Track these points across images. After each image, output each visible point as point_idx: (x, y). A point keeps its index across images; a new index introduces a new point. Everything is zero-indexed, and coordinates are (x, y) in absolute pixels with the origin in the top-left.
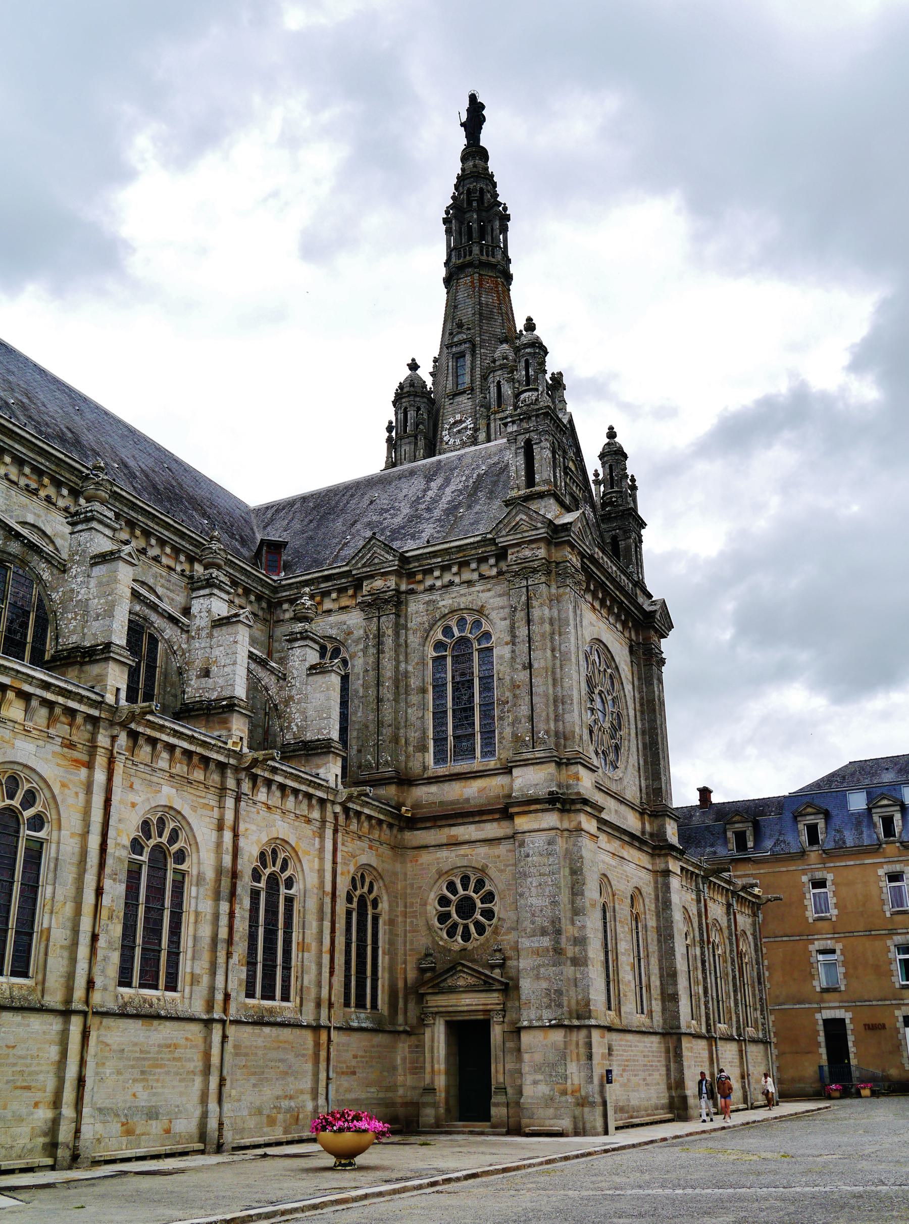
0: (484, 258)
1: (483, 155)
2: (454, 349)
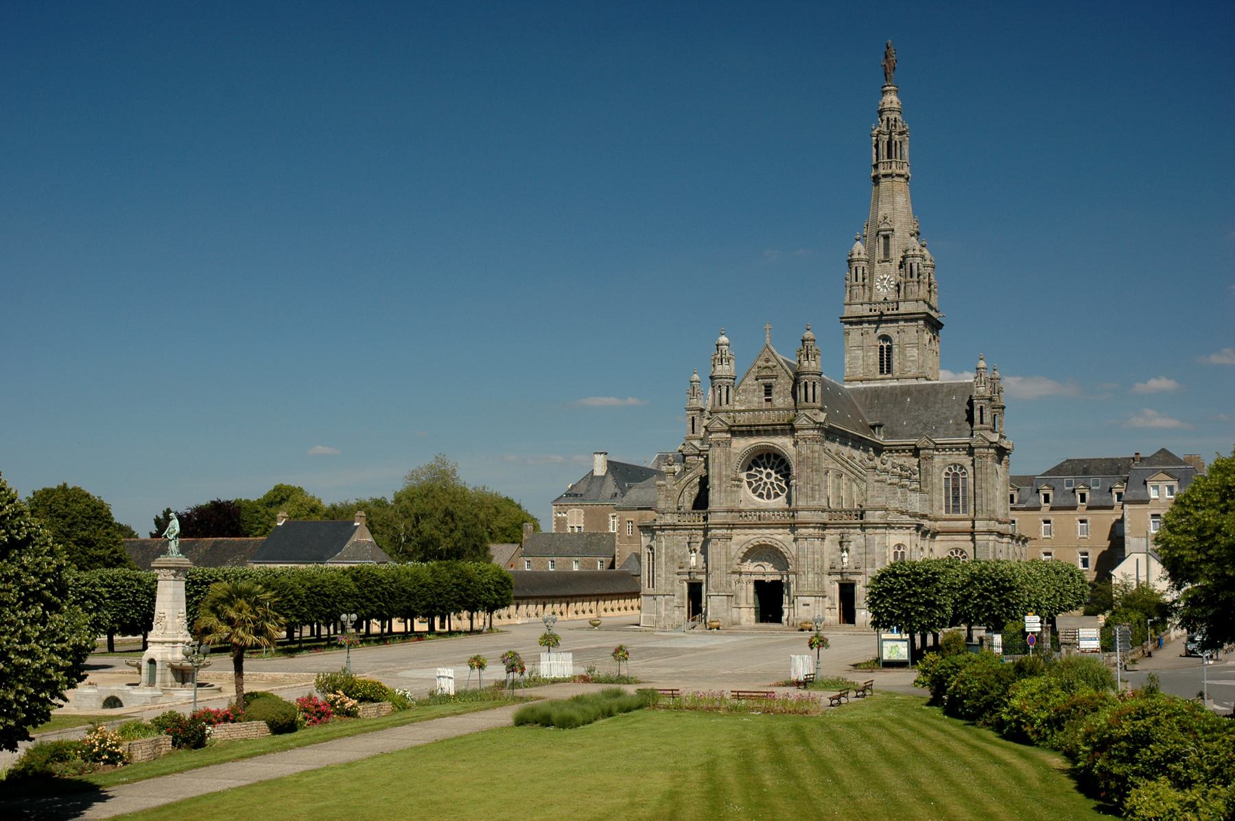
2: (883, 233)
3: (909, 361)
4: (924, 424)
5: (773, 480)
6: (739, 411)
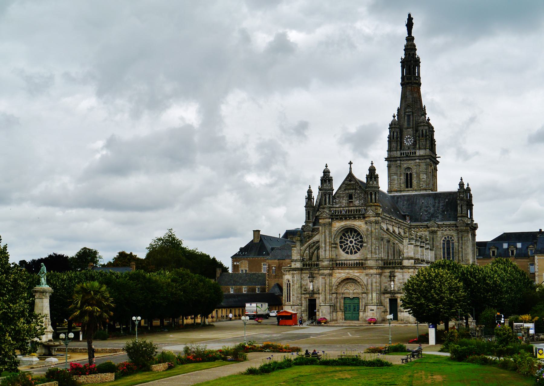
0: (415, 81)
1: (413, 39)
2: (407, 114)
3: (423, 181)
4: (431, 214)
5: (353, 244)
6: (336, 207)
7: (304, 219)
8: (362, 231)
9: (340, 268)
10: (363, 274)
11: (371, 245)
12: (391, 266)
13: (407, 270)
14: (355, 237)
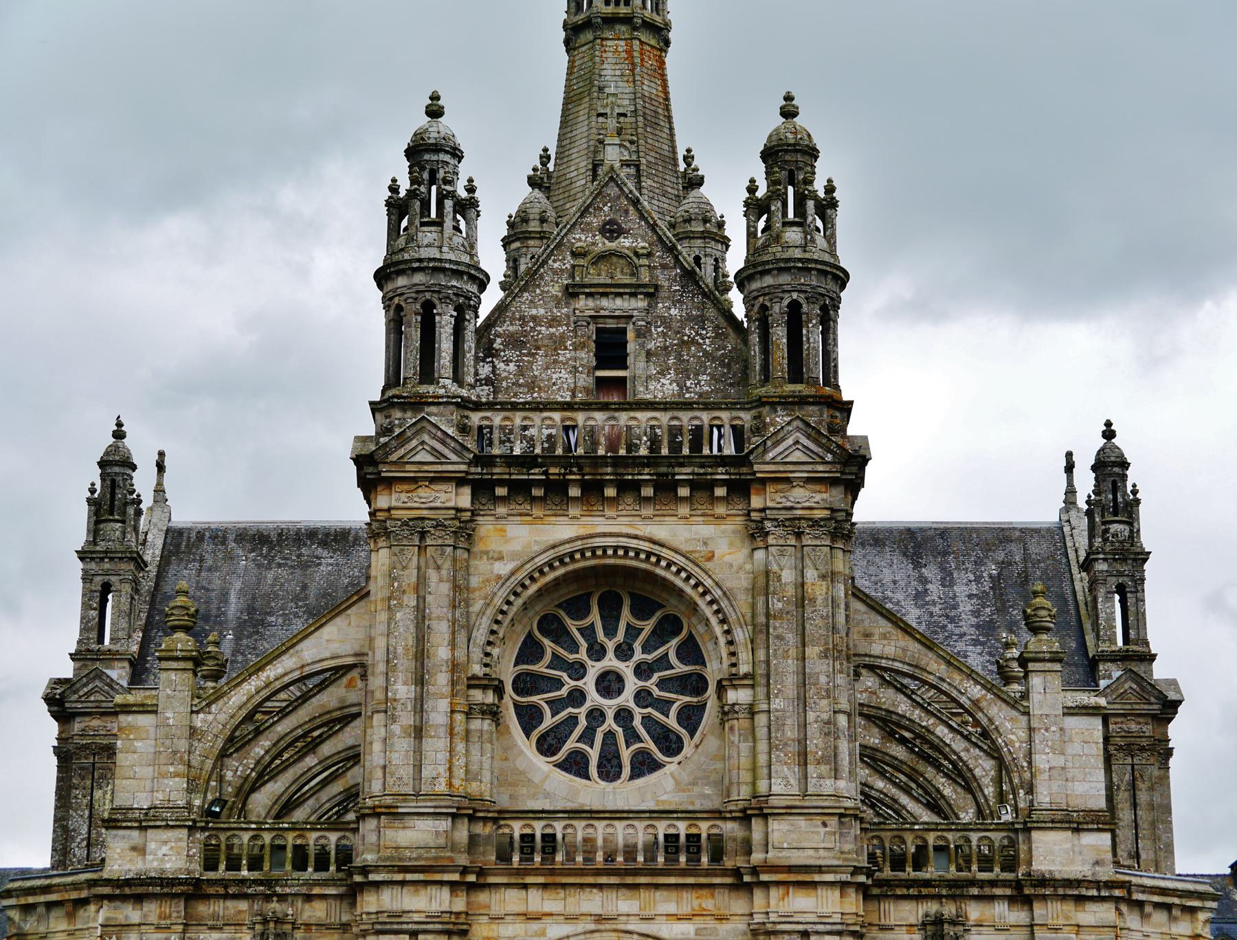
5: (627, 698)
7: (69, 636)
8: (718, 593)
9: (536, 872)
10: (725, 927)
11: (802, 701)
12: (910, 873)
13: (1069, 907)
14: (637, 646)
